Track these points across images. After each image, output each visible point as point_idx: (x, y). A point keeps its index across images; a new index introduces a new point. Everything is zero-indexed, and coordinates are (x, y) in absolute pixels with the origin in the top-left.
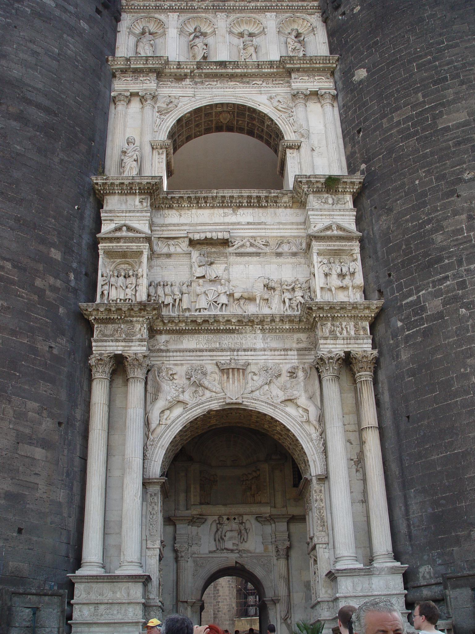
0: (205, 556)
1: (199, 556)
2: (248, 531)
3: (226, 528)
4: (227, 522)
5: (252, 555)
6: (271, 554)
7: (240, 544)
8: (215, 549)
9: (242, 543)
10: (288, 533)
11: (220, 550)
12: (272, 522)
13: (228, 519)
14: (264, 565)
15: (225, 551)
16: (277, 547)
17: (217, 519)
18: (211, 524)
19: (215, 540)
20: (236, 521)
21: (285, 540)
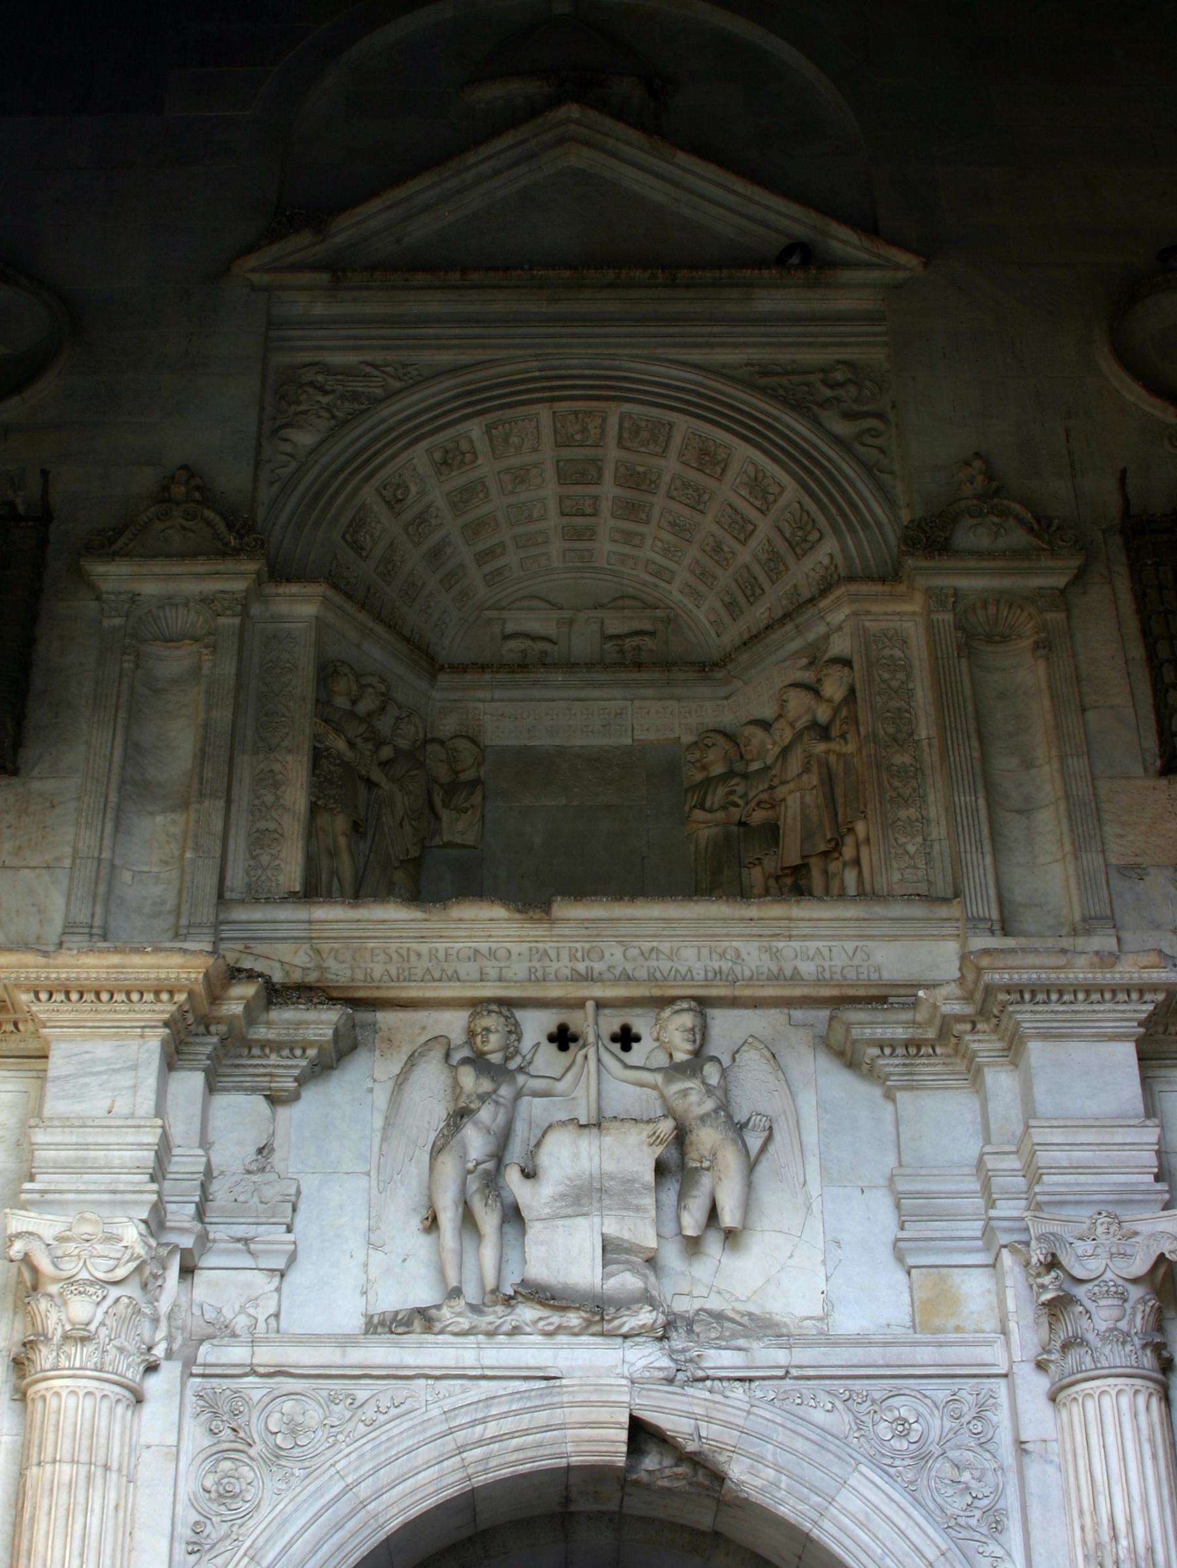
0: (327, 1356)
1: (266, 1356)
2: (754, 1141)
3: (535, 1109)
4: (548, 1059)
5: (803, 1356)
6: (984, 1354)
7: (672, 1257)
8: (423, 1294)
9: (693, 1246)
10: (1151, 1135)
11: (475, 1309)
12: (983, 1045)
13: (563, 1038)
14: (922, 1458)
15: (527, 1313)
16: (1053, 1264)
17: (457, 1036)
18: (401, 1081)
19: (432, 1223)
20: (638, 1054)
21: (1126, 1198)
